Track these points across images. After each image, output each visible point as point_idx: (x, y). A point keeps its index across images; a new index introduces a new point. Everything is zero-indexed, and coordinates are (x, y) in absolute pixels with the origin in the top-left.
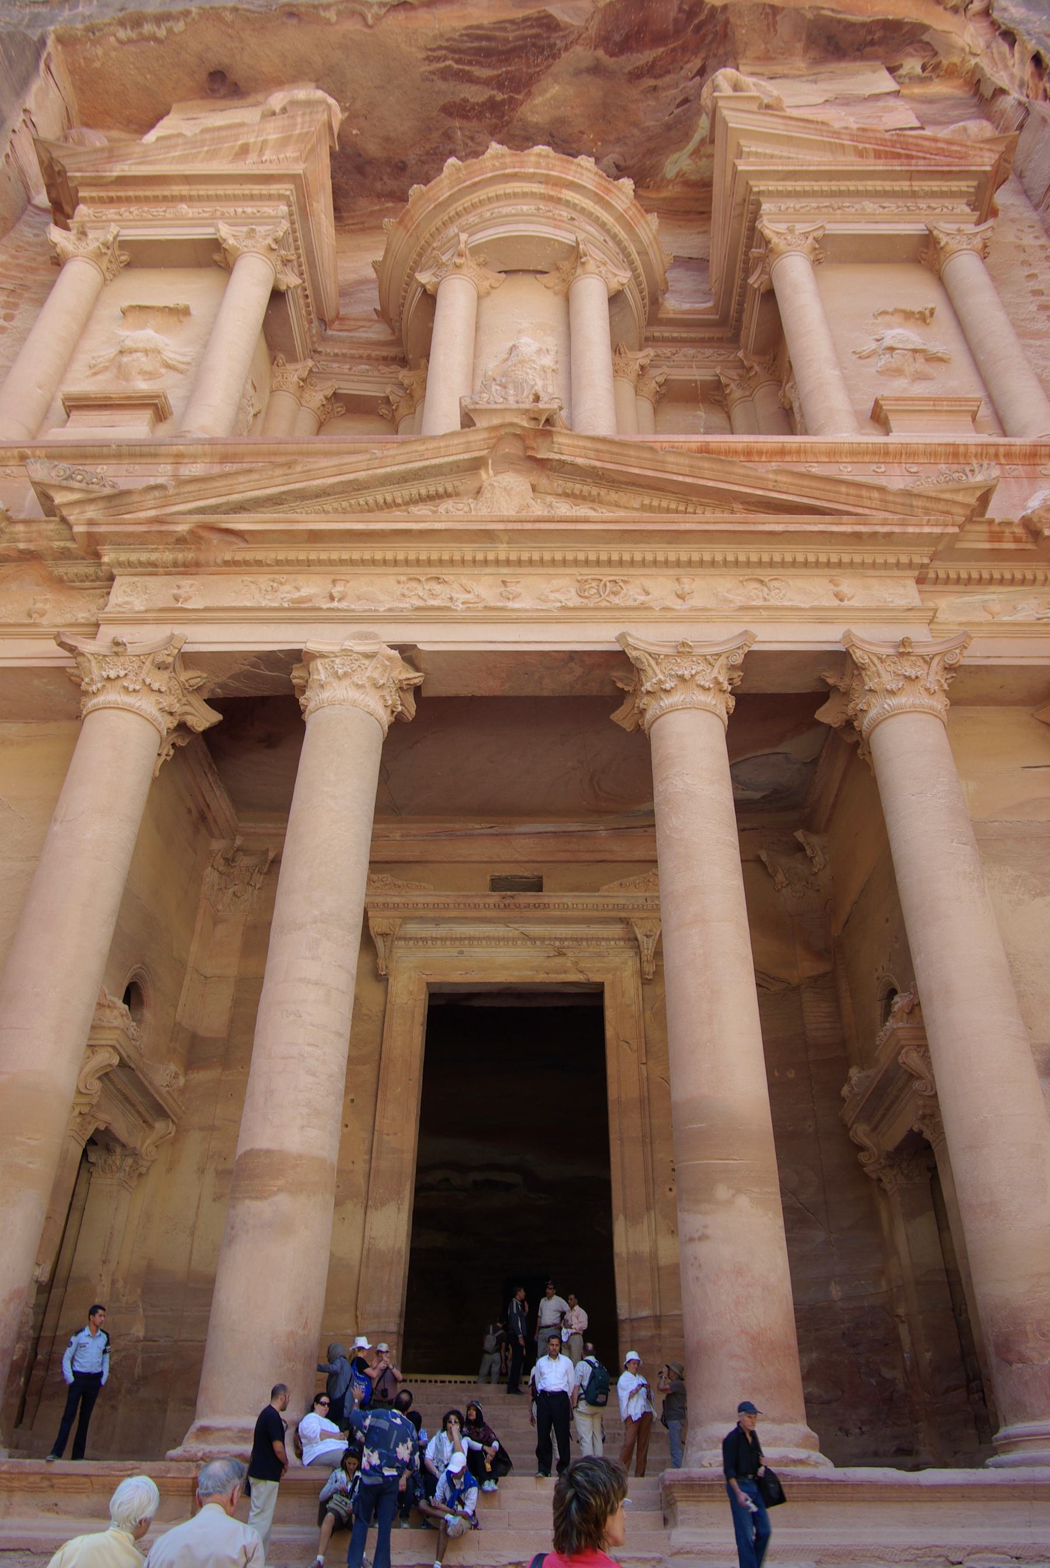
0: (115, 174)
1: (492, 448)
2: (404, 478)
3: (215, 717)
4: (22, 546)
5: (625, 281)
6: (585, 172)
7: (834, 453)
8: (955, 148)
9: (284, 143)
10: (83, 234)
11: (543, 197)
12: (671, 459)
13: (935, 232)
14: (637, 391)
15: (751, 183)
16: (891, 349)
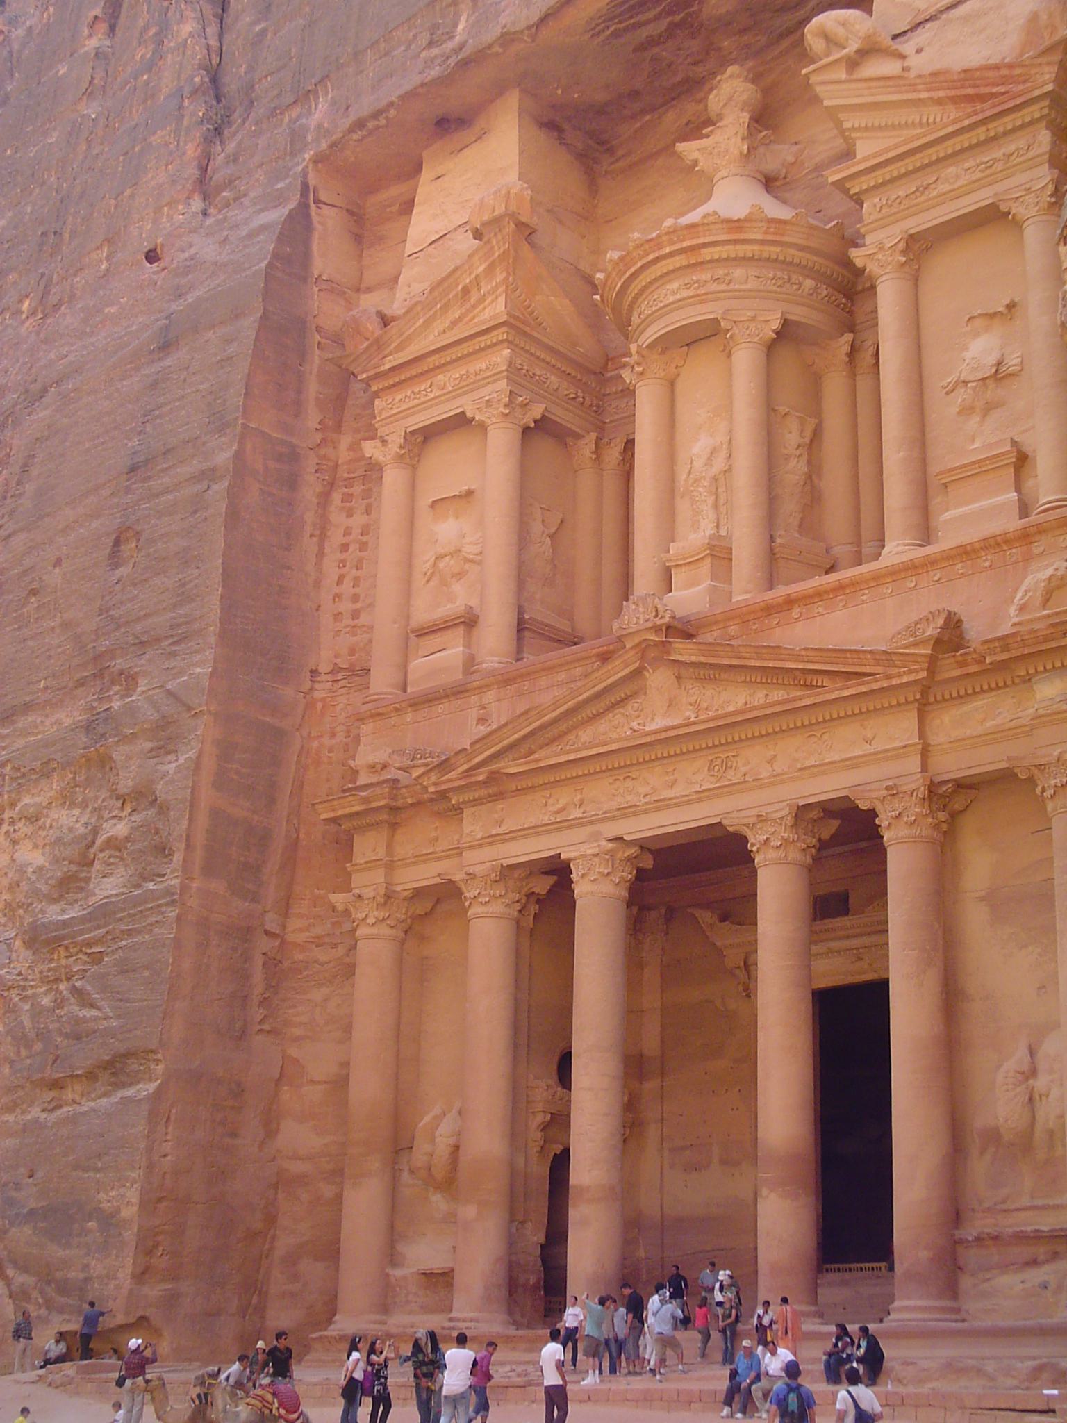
0: (387, 367)
1: (642, 658)
2: (597, 696)
3: (552, 880)
4: (410, 801)
5: (776, 325)
6: (712, 227)
7: (877, 579)
8: (1018, 71)
9: (490, 269)
10: (384, 442)
11: (688, 266)
12: (741, 649)
13: (1003, 207)
14: (853, 375)
15: (848, 185)
16: (965, 383)
